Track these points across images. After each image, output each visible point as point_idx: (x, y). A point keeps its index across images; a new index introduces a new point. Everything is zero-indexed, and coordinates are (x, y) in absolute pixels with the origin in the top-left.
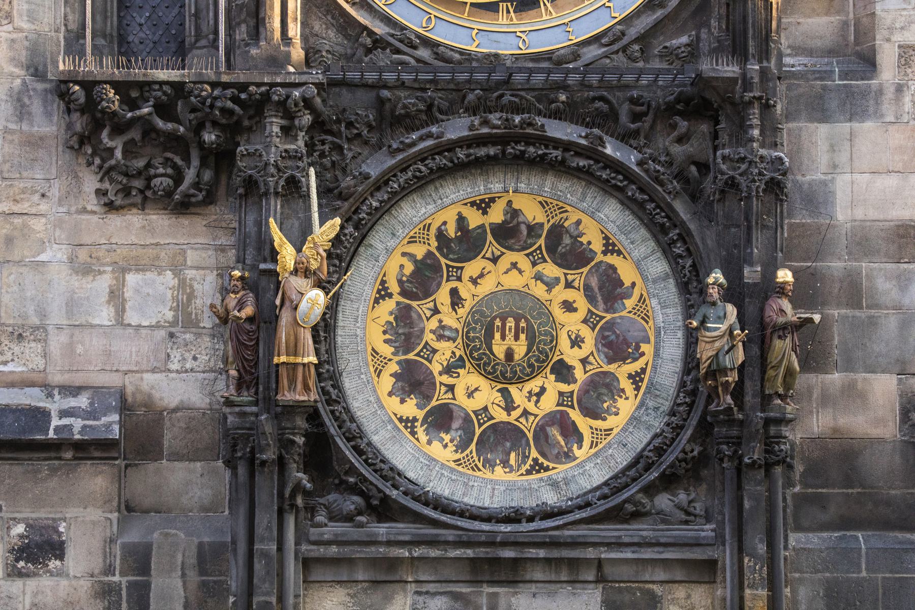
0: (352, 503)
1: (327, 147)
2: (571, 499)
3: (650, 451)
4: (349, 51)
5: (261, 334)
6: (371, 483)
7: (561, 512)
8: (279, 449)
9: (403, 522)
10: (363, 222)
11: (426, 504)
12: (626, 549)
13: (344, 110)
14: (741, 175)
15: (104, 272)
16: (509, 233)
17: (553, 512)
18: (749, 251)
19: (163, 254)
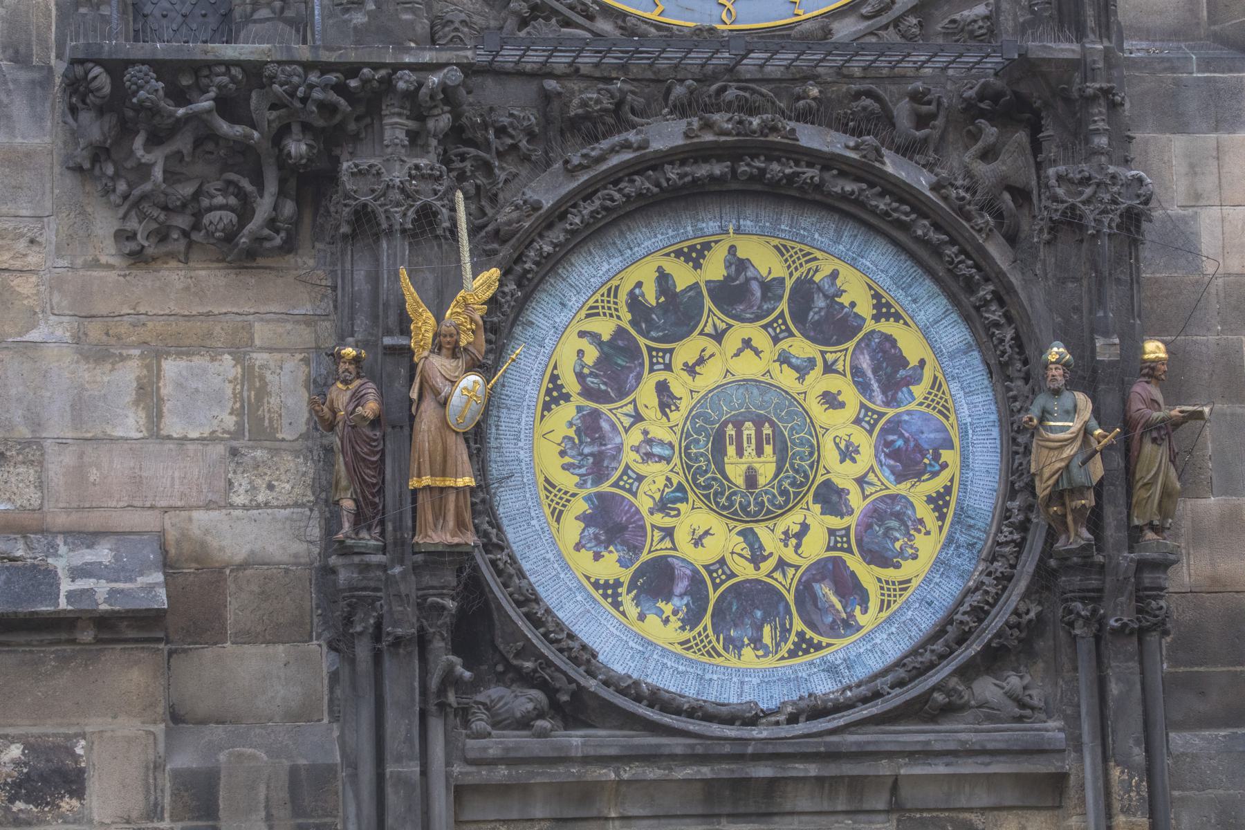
0: (525, 700)
1: (468, 165)
2: (850, 688)
3: (965, 613)
4: (493, 23)
5: (387, 442)
6: (558, 669)
7: (838, 708)
8: (418, 620)
9: (604, 728)
10: (529, 276)
11: (638, 699)
12: (937, 761)
13: (491, 109)
14: (1087, 202)
15: (129, 357)
16: (736, 293)
17: (825, 708)
18: (1101, 314)
19: (218, 329)
